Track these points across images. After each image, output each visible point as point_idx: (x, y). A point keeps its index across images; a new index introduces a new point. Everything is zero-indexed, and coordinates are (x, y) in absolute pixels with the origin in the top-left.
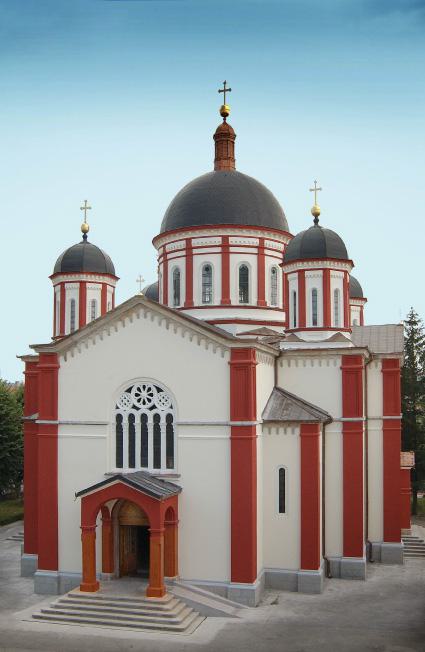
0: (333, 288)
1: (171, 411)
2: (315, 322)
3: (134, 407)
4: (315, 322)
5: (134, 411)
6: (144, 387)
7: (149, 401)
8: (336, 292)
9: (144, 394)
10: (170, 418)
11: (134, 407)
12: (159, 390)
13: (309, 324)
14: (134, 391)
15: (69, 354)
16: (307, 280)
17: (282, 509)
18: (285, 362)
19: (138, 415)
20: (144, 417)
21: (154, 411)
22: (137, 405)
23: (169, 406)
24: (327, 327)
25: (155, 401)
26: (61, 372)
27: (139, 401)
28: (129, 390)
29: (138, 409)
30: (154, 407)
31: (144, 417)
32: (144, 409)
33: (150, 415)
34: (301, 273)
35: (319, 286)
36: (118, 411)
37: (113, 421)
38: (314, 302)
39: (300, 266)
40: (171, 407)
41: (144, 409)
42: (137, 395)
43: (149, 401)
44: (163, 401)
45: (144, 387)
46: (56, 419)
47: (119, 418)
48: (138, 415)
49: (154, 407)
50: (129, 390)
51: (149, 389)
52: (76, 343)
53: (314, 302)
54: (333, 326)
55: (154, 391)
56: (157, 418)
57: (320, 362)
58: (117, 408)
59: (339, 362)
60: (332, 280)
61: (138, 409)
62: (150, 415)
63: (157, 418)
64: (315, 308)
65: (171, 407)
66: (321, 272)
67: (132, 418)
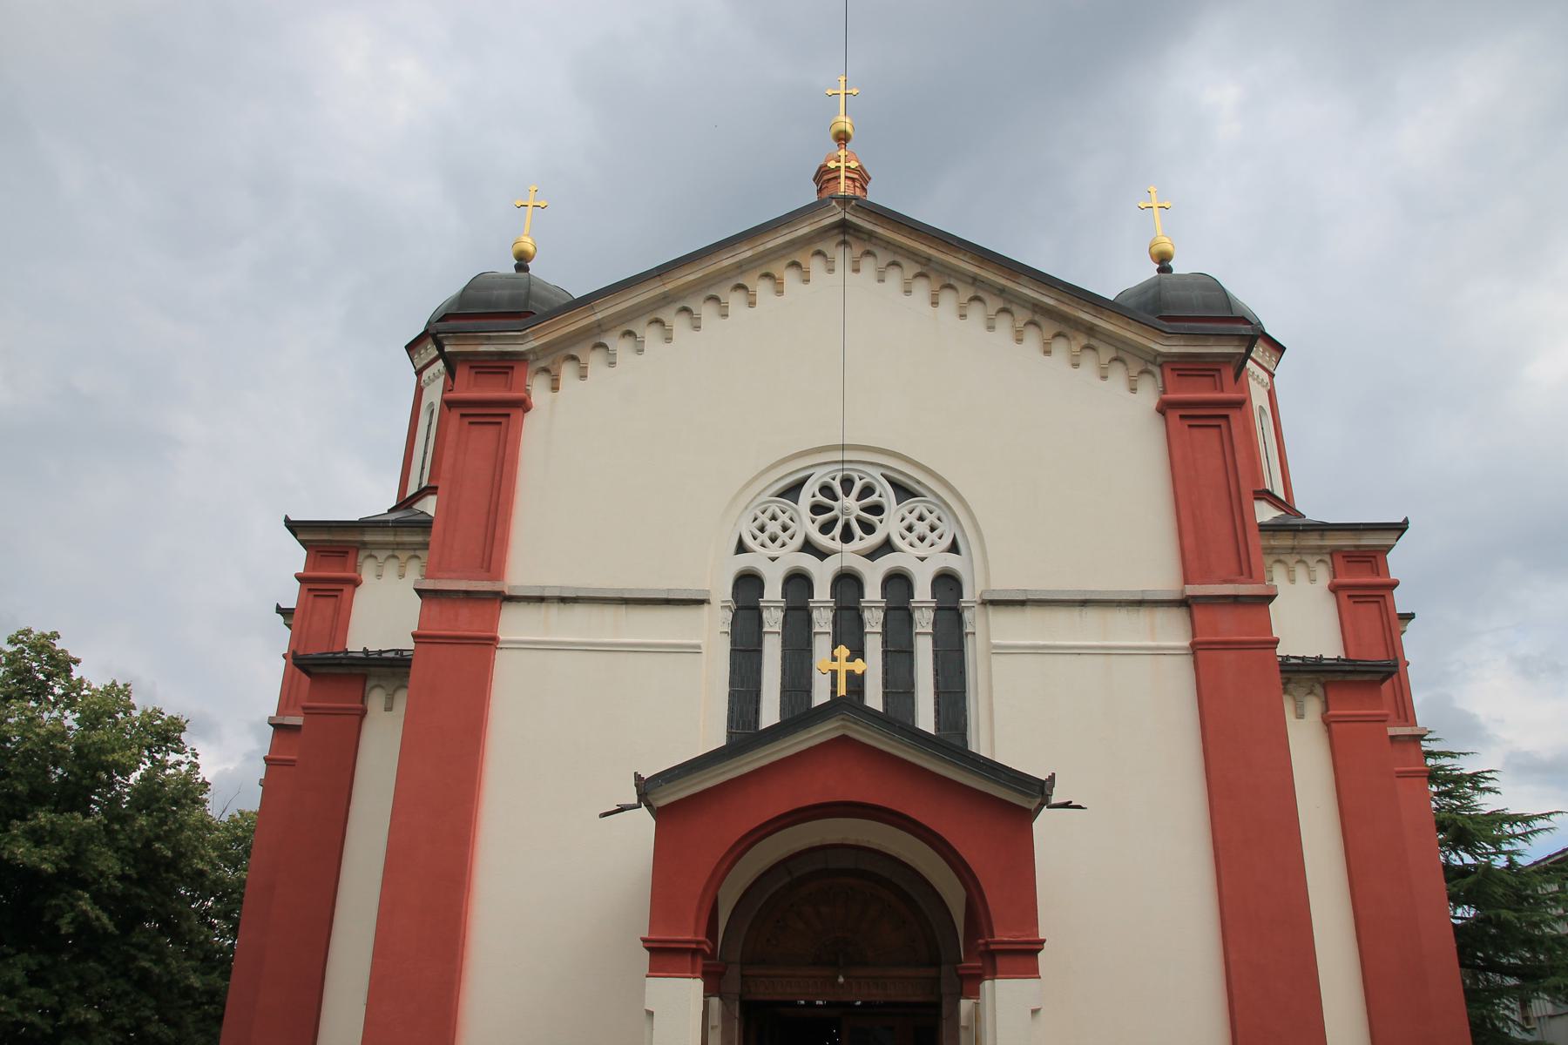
1: (952, 562)
3: (808, 547)
5: (808, 562)
6: (847, 483)
9: (849, 506)
10: (947, 582)
11: (808, 547)
12: (903, 491)
14: (807, 496)
15: (567, 372)
19: (822, 574)
20: (848, 582)
21: (887, 562)
22: (823, 541)
23: (947, 542)
25: (890, 525)
27: (826, 528)
28: (792, 491)
29: (822, 554)
30: (887, 546)
31: (848, 582)
32: (848, 556)
33: (873, 576)
36: (744, 561)
37: (722, 591)
40: (954, 548)
41: (848, 556)
42: (817, 509)
44: (922, 528)
45: (847, 483)
46: (498, 575)
47: (748, 583)
48: (822, 574)
49: (887, 546)
50: (792, 491)
51: (868, 490)
52: (601, 327)
55: (885, 494)
56: (898, 582)
58: (741, 548)
59: (1323, 576)
61: (822, 554)
62: (873, 576)
63: (898, 582)
65: (954, 548)
67: (798, 582)
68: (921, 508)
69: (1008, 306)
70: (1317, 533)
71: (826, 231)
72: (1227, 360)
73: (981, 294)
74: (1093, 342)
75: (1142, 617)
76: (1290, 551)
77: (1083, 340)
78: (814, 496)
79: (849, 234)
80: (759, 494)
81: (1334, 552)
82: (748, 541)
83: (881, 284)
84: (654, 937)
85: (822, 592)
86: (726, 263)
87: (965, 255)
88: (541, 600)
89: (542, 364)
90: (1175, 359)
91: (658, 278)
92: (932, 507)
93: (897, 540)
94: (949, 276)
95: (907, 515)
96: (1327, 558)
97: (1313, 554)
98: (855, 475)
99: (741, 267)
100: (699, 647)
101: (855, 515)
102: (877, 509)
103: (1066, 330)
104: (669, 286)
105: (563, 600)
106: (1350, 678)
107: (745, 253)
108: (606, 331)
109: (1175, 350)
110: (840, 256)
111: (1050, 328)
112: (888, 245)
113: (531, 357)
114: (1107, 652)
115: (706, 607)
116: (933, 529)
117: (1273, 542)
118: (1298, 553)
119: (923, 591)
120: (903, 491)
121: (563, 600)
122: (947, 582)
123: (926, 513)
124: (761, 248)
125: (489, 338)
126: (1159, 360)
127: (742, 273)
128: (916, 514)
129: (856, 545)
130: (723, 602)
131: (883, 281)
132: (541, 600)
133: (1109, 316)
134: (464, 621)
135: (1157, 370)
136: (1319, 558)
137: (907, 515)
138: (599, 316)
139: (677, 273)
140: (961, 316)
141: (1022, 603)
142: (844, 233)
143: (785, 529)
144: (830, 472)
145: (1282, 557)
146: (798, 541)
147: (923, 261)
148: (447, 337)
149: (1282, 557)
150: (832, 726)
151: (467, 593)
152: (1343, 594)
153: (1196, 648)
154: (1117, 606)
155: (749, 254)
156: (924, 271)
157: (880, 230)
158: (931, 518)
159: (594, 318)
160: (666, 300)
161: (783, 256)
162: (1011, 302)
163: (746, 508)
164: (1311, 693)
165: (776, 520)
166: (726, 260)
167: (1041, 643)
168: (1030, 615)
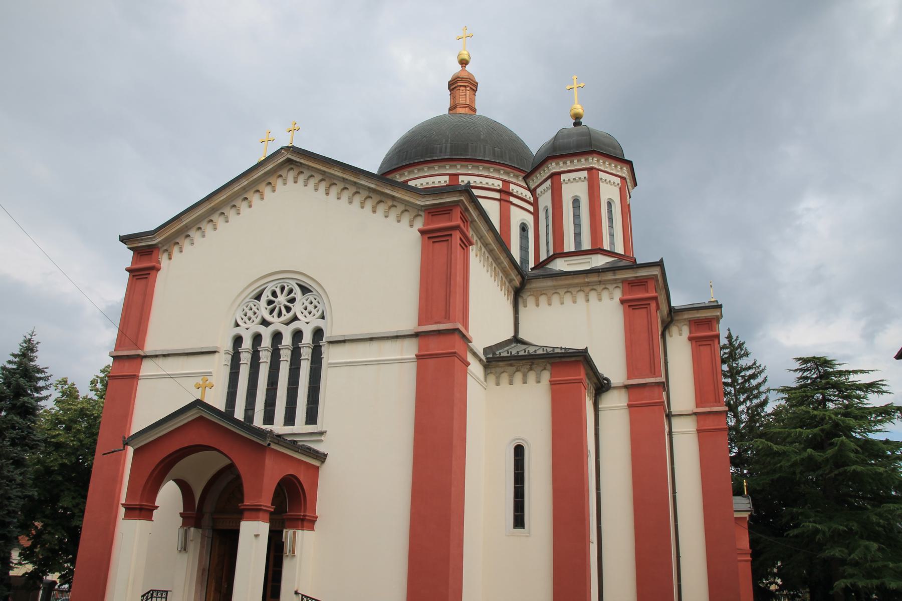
5: (262, 329)
7: (288, 309)
8: (609, 204)
9: (282, 299)
10: (318, 333)
12: (305, 290)
13: (569, 245)
14: (264, 298)
16: (564, 186)
17: (519, 521)
18: (531, 301)
19: (266, 334)
20: (277, 337)
21: (295, 325)
22: (268, 318)
24: (597, 250)
25: (297, 308)
26: (161, 277)
27: (271, 312)
30: (295, 318)
31: (277, 337)
32: (277, 324)
36: (237, 331)
37: (229, 345)
38: (577, 216)
41: (277, 324)
42: (270, 302)
43: (288, 309)
45: (283, 289)
46: (141, 347)
47: (238, 340)
50: (258, 297)
52: (187, 228)
53: (577, 216)
54: (606, 247)
56: (298, 335)
57: (587, 296)
58: (237, 325)
59: (618, 294)
63: (298, 335)
64: (577, 225)
67: (257, 338)
68: (311, 298)
69: (358, 190)
70: (611, 272)
71: (282, 165)
72: (456, 204)
73: (347, 186)
74: (395, 203)
75: (397, 344)
76: (599, 283)
77: (390, 203)
78: (268, 297)
79: (293, 164)
80: (245, 298)
81: (624, 281)
82: (240, 322)
83: (306, 187)
84: (127, 503)
85: (266, 342)
86: (236, 189)
87: (337, 168)
88: (156, 356)
89: (165, 248)
90: (430, 207)
91: (207, 201)
92: (316, 297)
93: (299, 316)
94: (334, 179)
95: (305, 301)
96: (620, 285)
97: (612, 284)
98: (285, 285)
99: (245, 189)
100: (211, 373)
101: (283, 304)
102: (292, 300)
103: (383, 199)
104: (212, 204)
105: (164, 356)
106: (564, 360)
107: (244, 182)
108: (190, 228)
109: (427, 203)
110: (291, 176)
111: (376, 198)
112: (309, 168)
113: (160, 245)
114: (378, 363)
115: (217, 354)
116: (316, 307)
117: (586, 280)
118: (604, 284)
119: (307, 338)
120: (305, 290)
121: (164, 356)
122: (318, 333)
123: (313, 300)
124: (251, 179)
125: (142, 240)
126: (423, 208)
127: (246, 191)
128: (309, 300)
129: (283, 318)
130: (225, 351)
131: (306, 186)
132: (156, 356)
133: (398, 190)
134: (126, 369)
135: (422, 214)
136: (615, 285)
137: (305, 301)
138: (184, 223)
139: (215, 198)
140: (338, 198)
141: (344, 341)
142: (291, 164)
143: (255, 313)
144: (275, 285)
145: (595, 287)
146: (259, 319)
147: (323, 173)
148: (127, 242)
149: (595, 287)
150: (194, 412)
151: (128, 356)
152: (627, 305)
153: (419, 357)
154: (387, 339)
155: (246, 182)
156: (324, 178)
157: (302, 161)
158: (315, 302)
159: (182, 224)
160: (213, 210)
161: (264, 180)
162: (359, 188)
163: (239, 306)
164: (545, 369)
165: (251, 310)
166: (236, 188)
167: (343, 361)
168: (347, 347)
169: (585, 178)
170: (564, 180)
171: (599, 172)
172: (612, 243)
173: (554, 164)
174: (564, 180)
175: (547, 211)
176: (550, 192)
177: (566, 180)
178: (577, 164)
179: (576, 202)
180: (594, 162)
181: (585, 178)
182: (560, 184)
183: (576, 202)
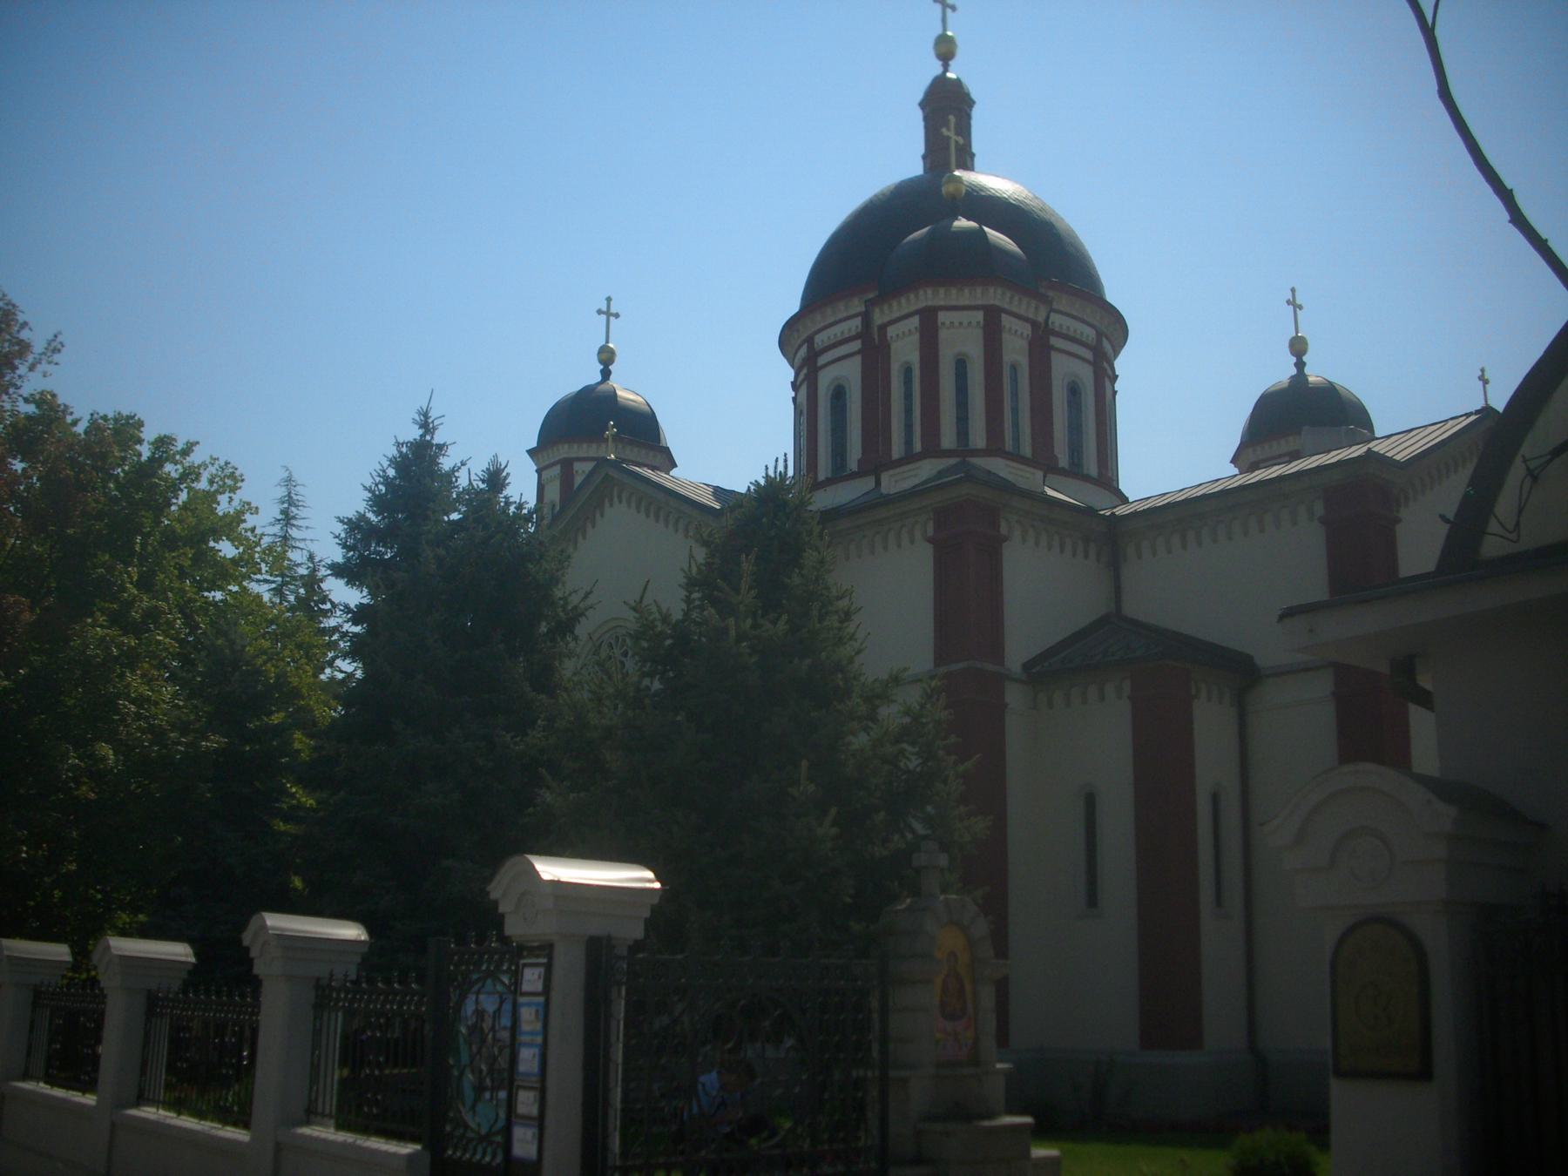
0: (1008, 358)
2: (963, 433)
4: (963, 433)
13: (948, 440)
34: (928, 319)
35: (974, 350)
39: (927, 297)
60: (1006, 336)
66: (979, 316)
169: (978, 323)
170: (943, 324)
171: (1003, 315)
172: (1016, 439)
173: (929, 292)
174: (943, 324)
175: (908, 371)
176: (916, 338)
177: (948, 323)
178: (965, 297)
179: (961, 365)
180: (995, 296)
181: (978, 323)
182: (936, 330)
183: (961, 365)
